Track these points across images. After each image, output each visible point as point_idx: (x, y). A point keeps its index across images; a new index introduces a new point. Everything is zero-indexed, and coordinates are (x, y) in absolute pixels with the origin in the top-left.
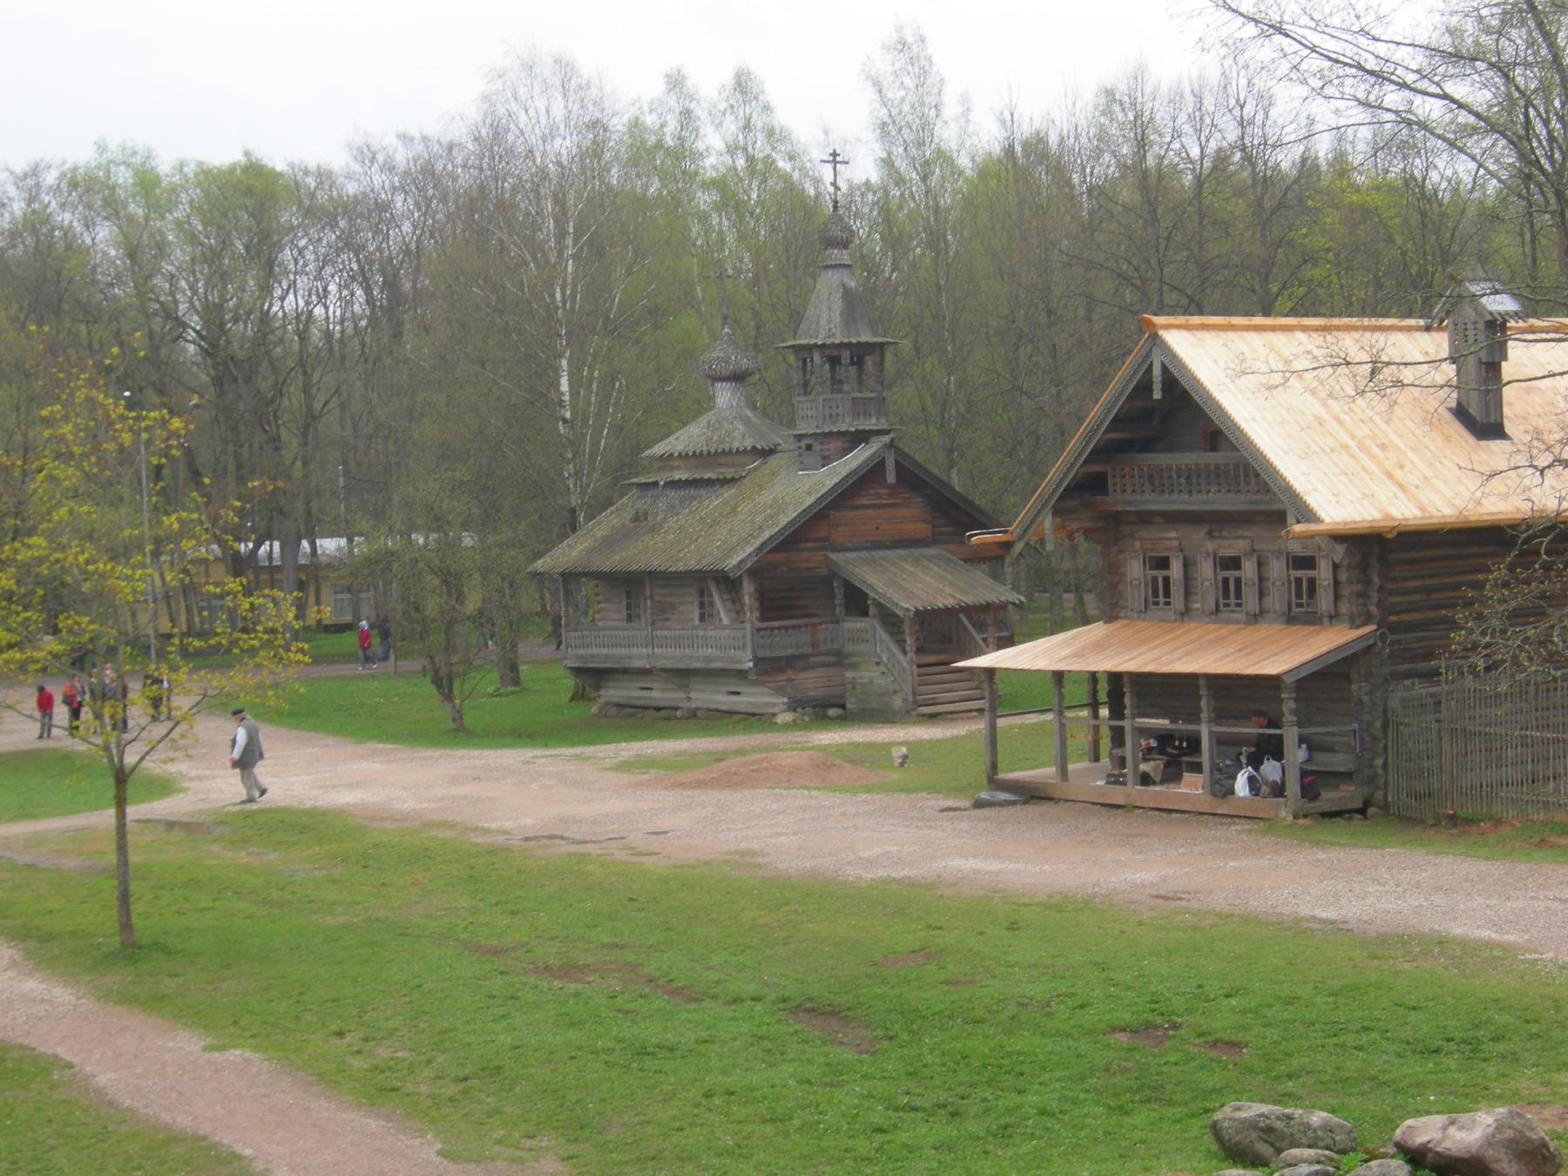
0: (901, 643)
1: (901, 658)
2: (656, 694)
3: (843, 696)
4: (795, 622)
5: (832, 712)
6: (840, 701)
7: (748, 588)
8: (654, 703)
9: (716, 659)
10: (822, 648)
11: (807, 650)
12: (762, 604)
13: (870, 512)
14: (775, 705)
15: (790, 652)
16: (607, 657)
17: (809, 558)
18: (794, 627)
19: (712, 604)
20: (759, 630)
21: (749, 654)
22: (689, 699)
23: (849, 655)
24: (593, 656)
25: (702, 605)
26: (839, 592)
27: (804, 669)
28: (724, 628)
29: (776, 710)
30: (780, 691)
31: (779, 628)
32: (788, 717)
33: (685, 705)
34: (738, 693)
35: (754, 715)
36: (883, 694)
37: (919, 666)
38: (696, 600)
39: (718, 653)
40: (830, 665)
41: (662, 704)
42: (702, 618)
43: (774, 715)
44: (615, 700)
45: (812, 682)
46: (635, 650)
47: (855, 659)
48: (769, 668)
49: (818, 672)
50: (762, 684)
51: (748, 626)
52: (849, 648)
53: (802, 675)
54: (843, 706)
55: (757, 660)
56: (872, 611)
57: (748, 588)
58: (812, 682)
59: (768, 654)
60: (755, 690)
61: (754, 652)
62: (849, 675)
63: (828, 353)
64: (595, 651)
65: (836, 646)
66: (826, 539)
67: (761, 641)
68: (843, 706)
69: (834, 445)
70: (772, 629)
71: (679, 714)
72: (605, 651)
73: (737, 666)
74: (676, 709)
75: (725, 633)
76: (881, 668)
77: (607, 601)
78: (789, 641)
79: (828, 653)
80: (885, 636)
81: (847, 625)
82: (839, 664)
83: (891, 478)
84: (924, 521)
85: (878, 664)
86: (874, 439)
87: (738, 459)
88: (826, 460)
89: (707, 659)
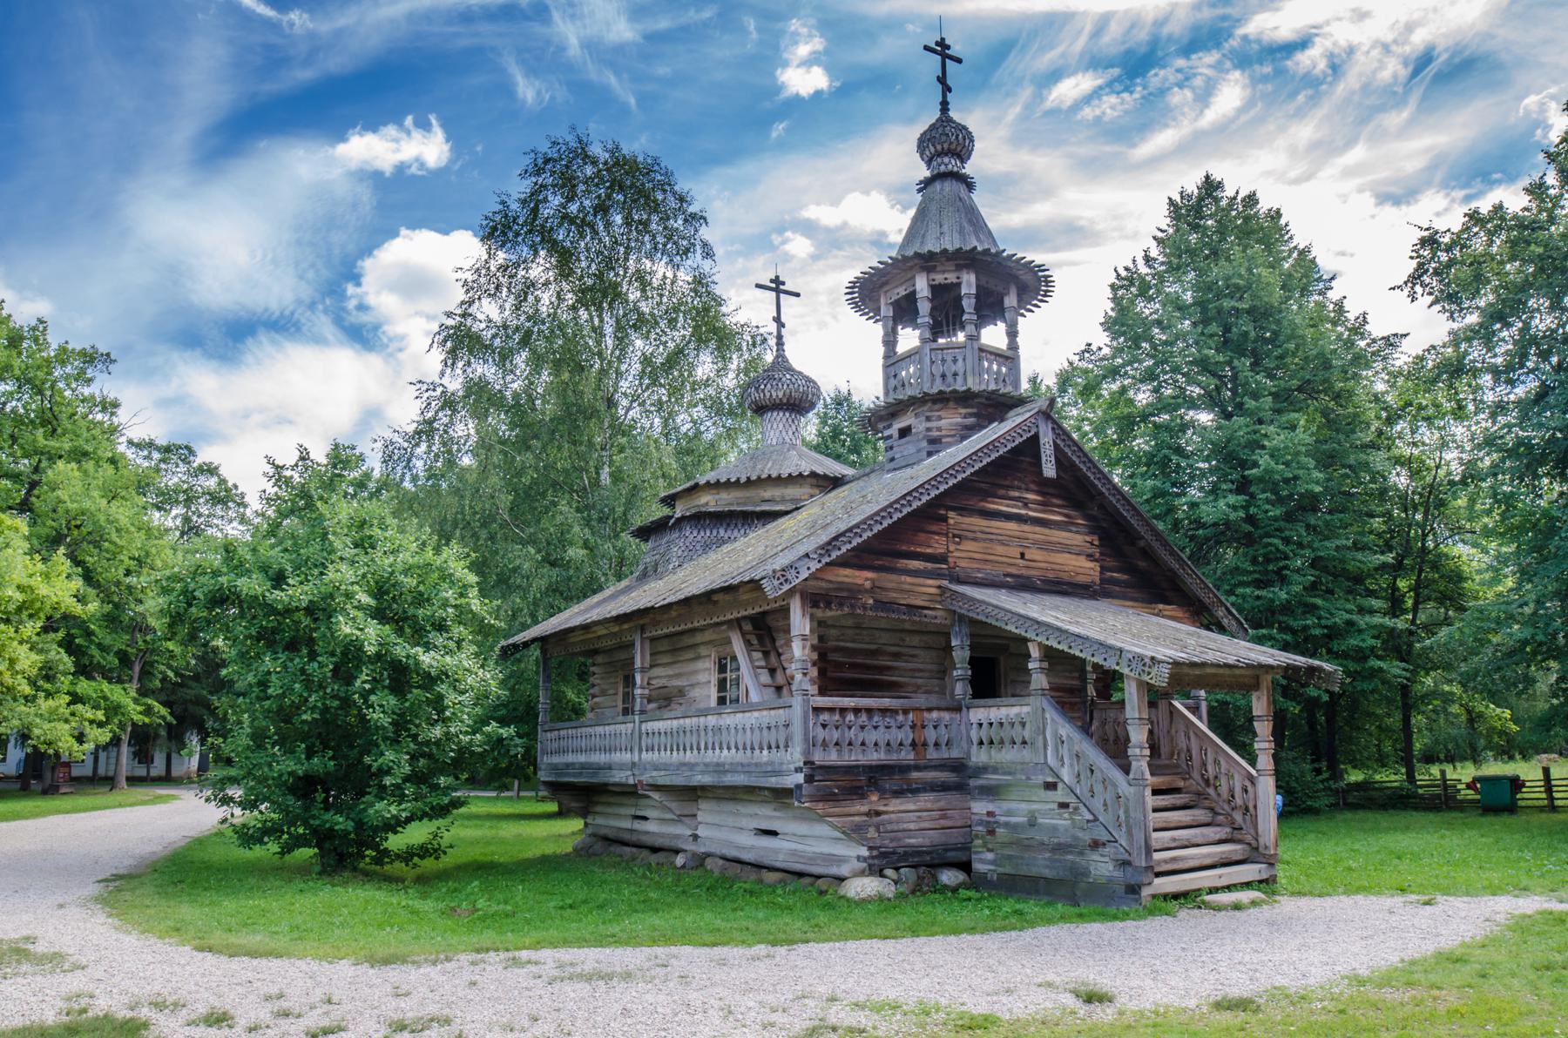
0: (1117, 749)
1: (1116, 774)
2: (650, 827)
3: (966, 848)
4: (886, 702)
5: (949, 877)
6: (962, 857)
7: (800, 621)
8: (646, 839)
9: (734, 768)
10: (932, 754)
11: (907, 756)
12: (822, 673)
13: (1012, 526)
14: (841, 860)
15: (875, 757)
16: (584, 766)
17: (916, 587)
18: (884, 711)
19: (737, 682)
20: (817, 710)
21: (796, 755)
22: (695, 837)
23: (983, 769)
24: (568, 765)
25: (722, 685)
26: (961, 653)
27: (898, 793)
28: (752, 708)
29: (844, 870)
30: (855, 833)
31: (857, 711)
32: (866, 886)
33: (690, 847)
34: (774, 833)
35: (800, 875)
36: (1060, 848)
37: (1155, 792)
38: (714, 678)
39: (739, 757)
40: (944, 788)
41: (658, 842)
42: (722, 701)
43: (841, 879)
44: (603, 832)
45: (912, 818)
46: (617, 757)
47: (992, 778)
48: (838, 786)
49: (926, 800)
50: (821, 818)
51: (797, 702)
52: (979, 757)
53: (895, 805)
54: (965, 867)
55: (813, 771)
56: (1039, 680)
57: (800, 621)
58: (912, 818)
59: (833, 757)
60: (802, 828)
61: (807, 752)
62: (980, 807)
63: (939, 278)
64: (570, 758)
65: (955, 753)
66: (942, 559)
67: (821, 734)
68: (965, 867)
69: (950, 419)
70: (843, 711)
71: (680, 860)
72: (582, 758)
73: (773, 782)
74: (677, 852)
75: (752, 718)
76: (1060, 795)
77: (603, 693)
78: (875, 739)
79: (942, 766)
80: (1066, 730)
81: (978, 714)
82: (960, 788)
83: (1049, 470)
84: (1090, 557)
85: (1051, 786)
86: (1019, 410)
87: (792, 492)
88: (935, 444)
89: (719, 768)
